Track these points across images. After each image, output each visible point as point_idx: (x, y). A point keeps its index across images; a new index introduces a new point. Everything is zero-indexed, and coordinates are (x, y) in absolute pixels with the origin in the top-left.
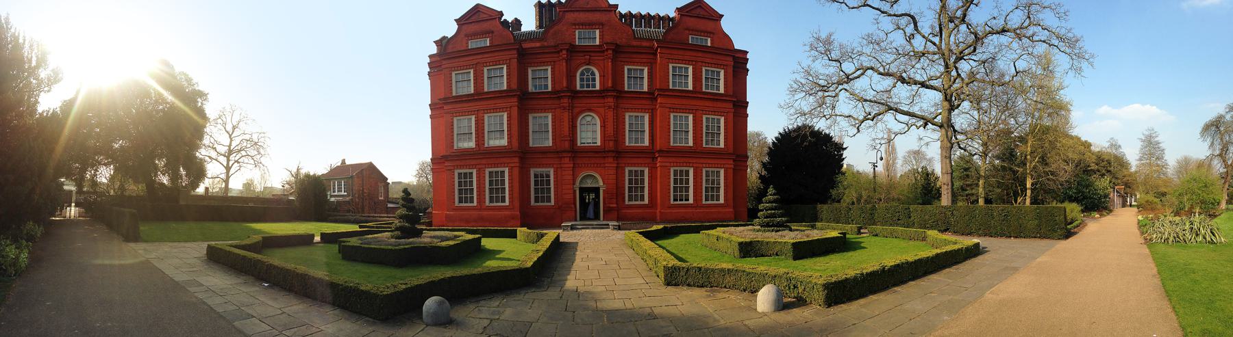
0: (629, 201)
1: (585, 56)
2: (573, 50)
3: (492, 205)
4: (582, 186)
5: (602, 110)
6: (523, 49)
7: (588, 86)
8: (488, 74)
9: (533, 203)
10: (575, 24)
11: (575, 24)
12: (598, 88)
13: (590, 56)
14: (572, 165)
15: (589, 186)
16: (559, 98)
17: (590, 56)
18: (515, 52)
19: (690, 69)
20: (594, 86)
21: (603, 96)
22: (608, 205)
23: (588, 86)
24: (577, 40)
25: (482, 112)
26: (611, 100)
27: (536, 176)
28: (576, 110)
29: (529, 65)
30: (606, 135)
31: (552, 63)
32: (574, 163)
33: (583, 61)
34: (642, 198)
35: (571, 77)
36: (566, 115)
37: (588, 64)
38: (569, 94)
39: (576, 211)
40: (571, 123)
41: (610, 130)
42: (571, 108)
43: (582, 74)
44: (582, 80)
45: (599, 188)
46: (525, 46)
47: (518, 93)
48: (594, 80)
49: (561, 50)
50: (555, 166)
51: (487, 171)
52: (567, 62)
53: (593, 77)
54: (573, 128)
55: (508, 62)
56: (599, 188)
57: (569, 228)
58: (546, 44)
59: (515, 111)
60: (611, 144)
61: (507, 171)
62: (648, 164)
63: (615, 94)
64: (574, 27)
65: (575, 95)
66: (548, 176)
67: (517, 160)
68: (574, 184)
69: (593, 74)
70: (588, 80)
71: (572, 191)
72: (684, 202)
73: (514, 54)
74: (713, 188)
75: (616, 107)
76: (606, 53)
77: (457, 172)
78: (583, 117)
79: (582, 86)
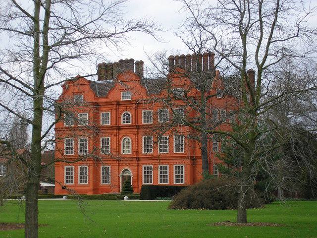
2: (118, 103)
3: (81, 184)
4: (124, 175)
26: (134, 130)
28: (120, 136)
35: (118, 118)
43: (124, 116)
51: (79, 167)
53: (126, 118)
54: (119, 145)
58: (108, 100)
60: (135, 153)
61: (87, 167)
65: (119, 128)
69: (129, 115)
77: (65, 167)
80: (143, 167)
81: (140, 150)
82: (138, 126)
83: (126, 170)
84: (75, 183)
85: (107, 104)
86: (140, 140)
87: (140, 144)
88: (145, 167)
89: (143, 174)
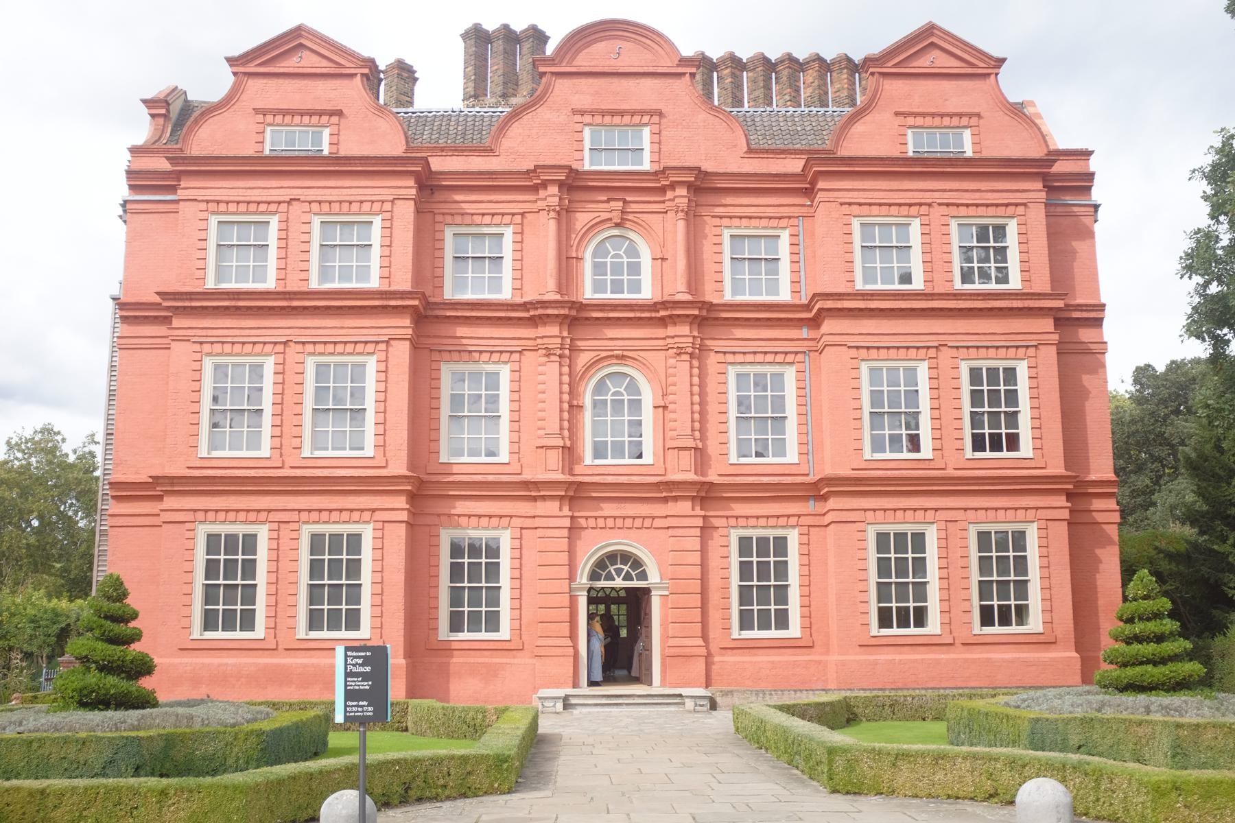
0: (742, 628)
1: (608, 201)
5: (657, 359)
6: (431, 174)
7: (617, 287)
8: (323, 236)
9: (444, 632)
10: (582, 113)
11: (582, 113)
12: (647, 293)
13: (625, 202)
14: (567, 522)
15: (619, 583)
16: (534, 321)
17: (625, 202)
18: (411, 182)
19: (915, 227)
20: (636, 287)
21: (662, 319)
22: (671, 642)
23: (617, 287)
24: (587, 153)
25: (299, 348)
27: (456, 550)
28: (583, 359)
29: (449, 219)
30: (670, 434)
31: (518, 219)
32: (572, 517)
33: (607, 215)
34: (782, 621)
35: (567, 265)
36: (551, 374)
37: (617, 225)
38: (562, 312)
39: (576, 656)
40: (566, 397)
41: (682, 419)
42: (567, 352)
43: (600, 251)
44: (599, 268)
45: (646, 592)
46: (437, 164)
47: (416, 303)
48: (635, 269)
49: (544, 185)
50: (517, 522)
52: (559, 221)
54: (575, 408)
55: (387, 206)
56: (646, 592)
57: (560, 706)
59: (401, 352)
60: (687, 459)
62: (799, 516)
63: (696, 312)
64: (578, 118)
66: (494, 551)
67: (401, 502)
68: (572, 578)
69: (633, 252)
70: (617, 268)
71: (565, 600)
72: (913, 630)
73: (408, 187)
74: (1003, 585)
75: (698, 354)
76: (670, 195)
78: (601, 382)
79: (598, 287)
80: (734, 536)
81: (713, 448)
82: (710, 306)
83: (612, 557)
84: (273, 628)
85: (491, 183)
86: (712, 387)
87: (712, 408)
88: (745, 543)
89: (735, 582)
